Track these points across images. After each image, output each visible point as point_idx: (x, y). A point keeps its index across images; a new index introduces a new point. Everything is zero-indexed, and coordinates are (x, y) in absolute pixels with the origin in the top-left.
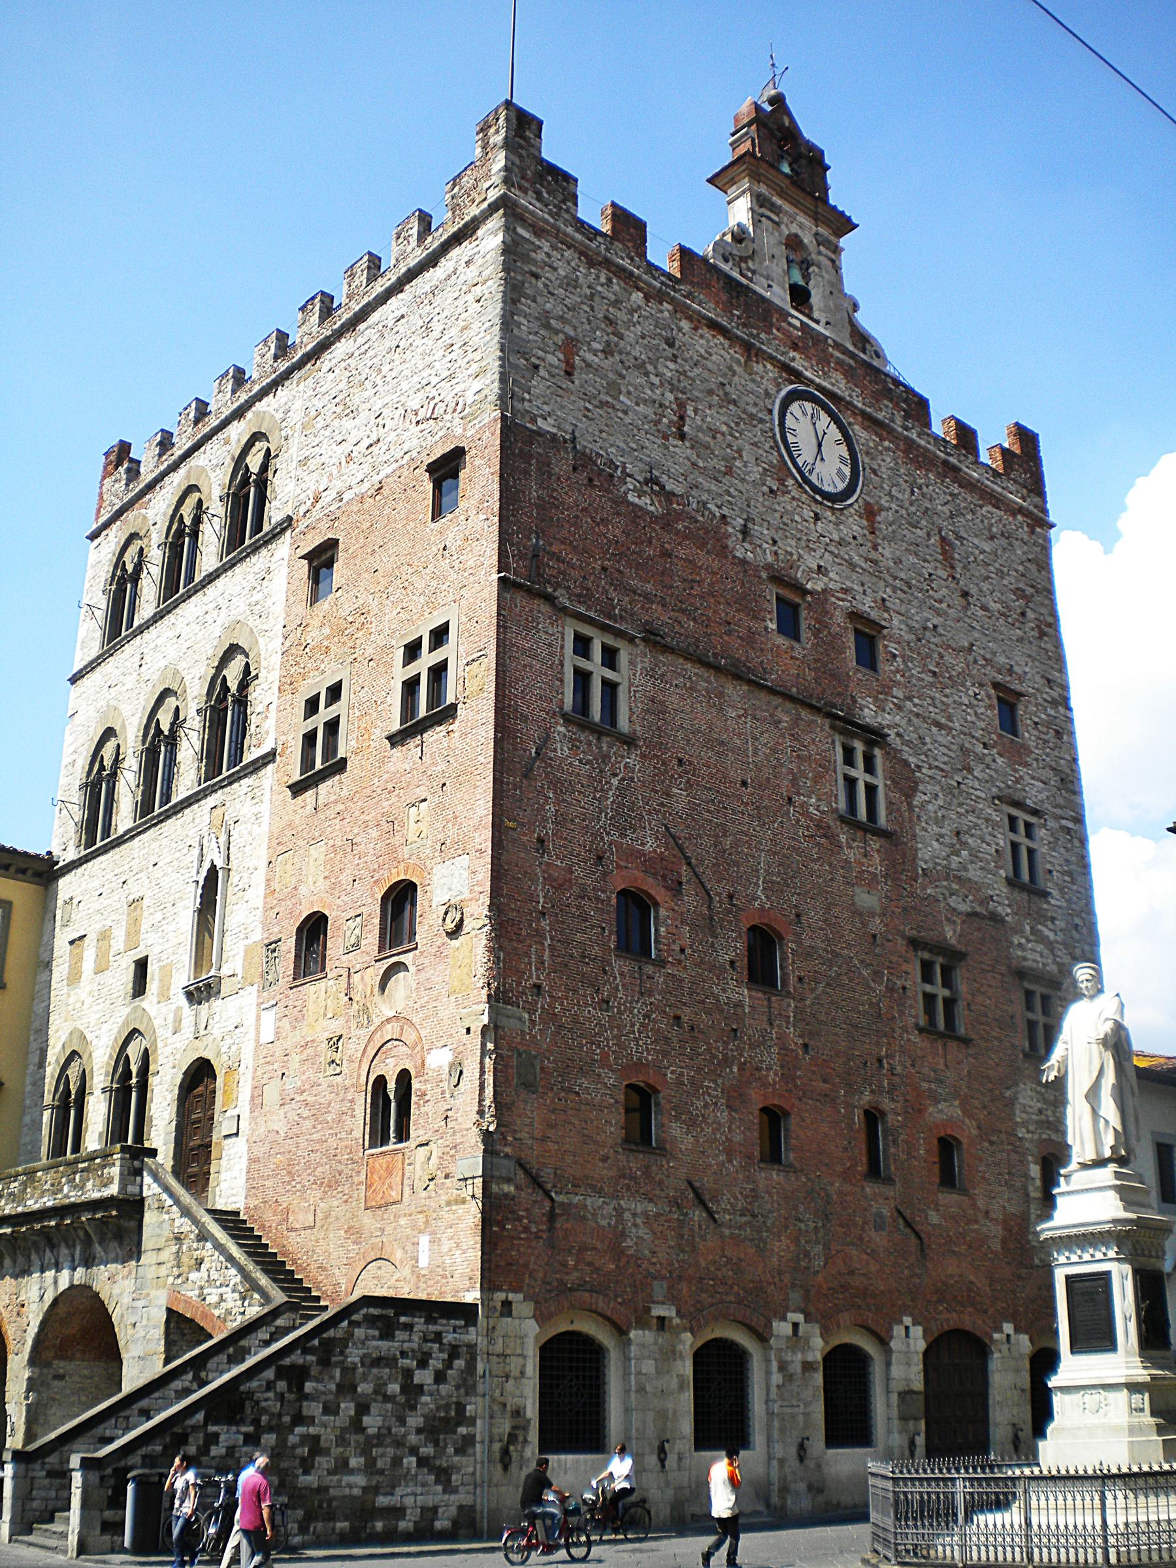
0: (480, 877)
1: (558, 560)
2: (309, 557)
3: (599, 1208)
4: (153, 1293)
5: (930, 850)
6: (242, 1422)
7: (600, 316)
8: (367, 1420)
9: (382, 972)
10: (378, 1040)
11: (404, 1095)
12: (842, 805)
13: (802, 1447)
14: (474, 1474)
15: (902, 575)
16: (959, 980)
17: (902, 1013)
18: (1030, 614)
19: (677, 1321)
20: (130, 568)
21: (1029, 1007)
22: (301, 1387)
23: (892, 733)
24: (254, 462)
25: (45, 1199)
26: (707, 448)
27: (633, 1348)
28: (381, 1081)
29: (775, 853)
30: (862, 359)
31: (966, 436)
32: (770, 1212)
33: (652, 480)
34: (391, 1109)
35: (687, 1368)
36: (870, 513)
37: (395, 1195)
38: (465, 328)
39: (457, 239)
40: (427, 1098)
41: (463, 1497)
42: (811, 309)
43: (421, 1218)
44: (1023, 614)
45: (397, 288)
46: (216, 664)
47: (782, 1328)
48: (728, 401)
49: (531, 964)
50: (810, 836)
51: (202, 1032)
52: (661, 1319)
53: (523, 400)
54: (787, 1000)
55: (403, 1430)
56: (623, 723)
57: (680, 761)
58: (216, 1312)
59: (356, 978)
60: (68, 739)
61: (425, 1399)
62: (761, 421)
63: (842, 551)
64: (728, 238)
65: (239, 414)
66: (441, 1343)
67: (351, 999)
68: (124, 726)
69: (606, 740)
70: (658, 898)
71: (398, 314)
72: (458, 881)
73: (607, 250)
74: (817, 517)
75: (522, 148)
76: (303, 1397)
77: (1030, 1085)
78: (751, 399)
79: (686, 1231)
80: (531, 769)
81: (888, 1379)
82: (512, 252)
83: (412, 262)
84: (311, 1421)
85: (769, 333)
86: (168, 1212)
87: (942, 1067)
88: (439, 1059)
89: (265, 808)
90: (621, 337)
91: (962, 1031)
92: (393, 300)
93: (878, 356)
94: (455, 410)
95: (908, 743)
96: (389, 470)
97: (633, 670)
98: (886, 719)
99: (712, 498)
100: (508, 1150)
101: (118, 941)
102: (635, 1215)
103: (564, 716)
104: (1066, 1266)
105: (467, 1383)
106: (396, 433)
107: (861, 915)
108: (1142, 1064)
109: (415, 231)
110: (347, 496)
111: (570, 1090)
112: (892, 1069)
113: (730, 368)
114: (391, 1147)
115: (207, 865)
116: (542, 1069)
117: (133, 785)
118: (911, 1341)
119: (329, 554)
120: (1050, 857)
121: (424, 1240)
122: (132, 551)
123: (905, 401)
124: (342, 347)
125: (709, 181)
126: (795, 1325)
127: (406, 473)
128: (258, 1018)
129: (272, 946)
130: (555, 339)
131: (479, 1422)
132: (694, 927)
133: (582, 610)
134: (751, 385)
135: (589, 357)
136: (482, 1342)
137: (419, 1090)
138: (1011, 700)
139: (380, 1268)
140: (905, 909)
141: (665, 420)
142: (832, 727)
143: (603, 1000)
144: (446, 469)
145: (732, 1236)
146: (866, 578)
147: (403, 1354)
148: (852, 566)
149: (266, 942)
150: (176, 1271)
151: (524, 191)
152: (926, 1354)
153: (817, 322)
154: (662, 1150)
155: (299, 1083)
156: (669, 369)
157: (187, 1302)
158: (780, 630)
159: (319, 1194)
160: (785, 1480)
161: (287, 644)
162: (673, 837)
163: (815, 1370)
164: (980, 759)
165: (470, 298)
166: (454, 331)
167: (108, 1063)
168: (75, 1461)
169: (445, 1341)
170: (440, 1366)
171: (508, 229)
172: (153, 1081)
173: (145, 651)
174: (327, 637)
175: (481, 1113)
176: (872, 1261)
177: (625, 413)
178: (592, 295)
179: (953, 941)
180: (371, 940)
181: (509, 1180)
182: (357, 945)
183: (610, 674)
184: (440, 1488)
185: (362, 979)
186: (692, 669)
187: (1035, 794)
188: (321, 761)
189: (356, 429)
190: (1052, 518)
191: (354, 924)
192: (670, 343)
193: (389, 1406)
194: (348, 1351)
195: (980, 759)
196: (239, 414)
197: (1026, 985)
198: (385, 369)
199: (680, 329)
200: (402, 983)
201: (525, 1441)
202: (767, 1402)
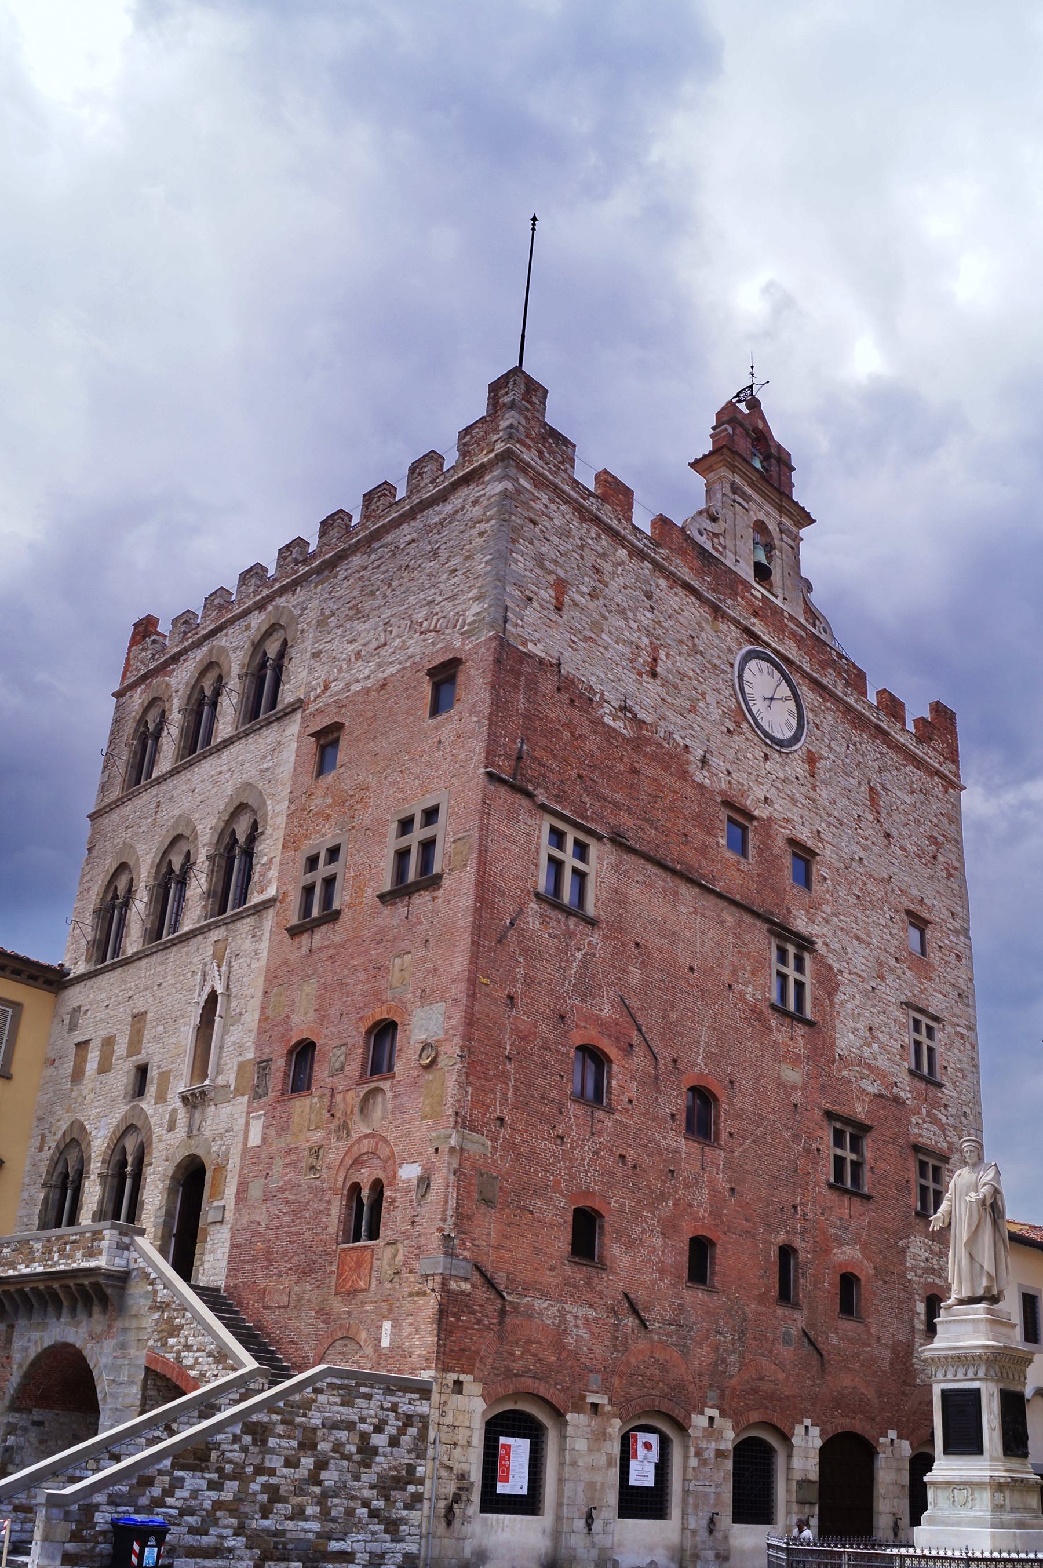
1: (539, 764)
3: (545, 1309)
6: (207, 1469)
9: (362, 1094)
11: (376, 1201)
13: (712, 1521)
16: (865, 1148)
17: (815, 1170)
19: (608, 1408)
27: (569, 1428)
29: (715, 1029)
32: (694, 1323)
40: (397, 1204)
49: (495, 1099)
50: (746, 1019)
52: (595, 1406)
54: (718, 1152)
58: (192, 1373)
59: (339, 1098)
66: (396, 1412)
67: (333, 1115)
70: (612, 1056)
77: (919, 1238)
79: (620, 1334)
80: (506, 937)
81: (789, 1469)
87: (847, 1217)
88: (410, 1172)
91: (866, 1190)
97: (600, 860)
99: (676, 728)
100: (466, 1253)
102: (576, 1317)
107: (785, 1087)
108: (1014, 1229)
111: (524, 1209)
116: (501, 1188)
118: (810, 1439)
130: (548, 578)
132: (642, 1084)
133: (559, 808)
135: (577, 597)
137: (390, 1197)
140: (822, 1086)
143: (558, 1136)
145: (660, 1342)
150: (156, 1336)
155: (281, 1183)
157: (165, 1362)
159: (294, 1278)
160: (696, 1548)
163: (726, 1457)
169: (400, 1411)
170: (395, 1432)
175: (444, 1220)
176: (779, 1370)
177: (606, 649)
180: (354, 1068)
200: (380, 1106)
202: (684, 1480)
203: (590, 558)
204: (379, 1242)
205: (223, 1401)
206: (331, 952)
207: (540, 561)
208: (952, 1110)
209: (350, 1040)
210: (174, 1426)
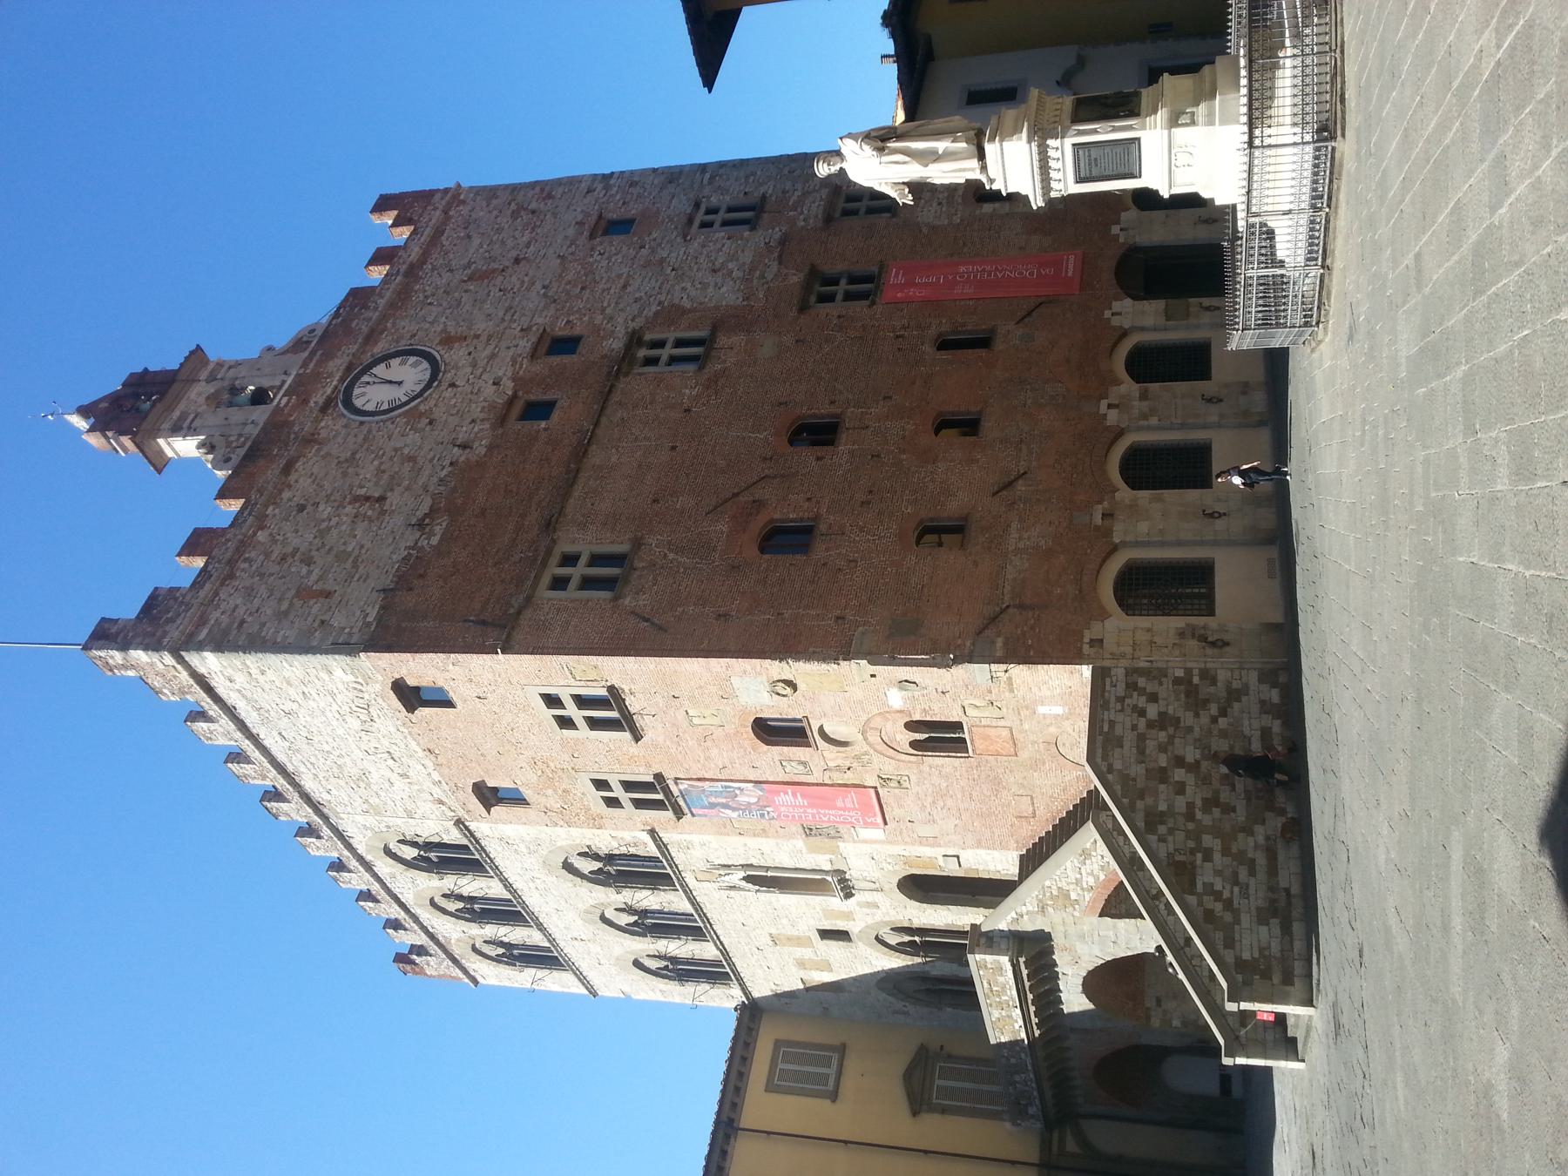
0: (749, 668)
2: (488, 809)
5: (727, 295)
7: (277, 568)
8: (1190, 759)
12: (690, 368)
13: (1210, 400)
14: (1232, 670)
15: (501, 314)
18: (533, 206)
20: (501, 951)
21: (855, 212)
22: (1162, 814)
23: (632, 325)
24: (410, 853)
26: (392, 477)
28: (915, 745)
30: (317, 344)
31: (382, 256)
33: (420, 525)
34: (939, 737)
35: (1144, 495)
36: (448, 341)
37: (1005, 733)
38: (289, 683)
39: (209, 690)
41: (1253, 678)
42: (272, 388)
43: (1024, 713)
44: (533, 212)
47: (1113, 417)
48: (352, 460)
53: (350, 634)
55: (1197, 729)
56: (623, 548)
57: (655, 501)
58: (1102, 877)
59: (831, 764)
60: (642, 996)
61: (1171, 711)
62: (369, 431)
63: (481, 363)
64: (210, 457)
65: (368, 867)
68: (631, 953)
69: (638, 564)
71: (278, 738)
72: (752, 684)
73: (219, 562)
74: (453, 385)
75: (125, 637)
76: (1171, 811)
78: (351, 439)
81: (1155, 329)
82: (221, 644)
83: (232, 727)
84: (1190, 806)
85: (293, 424)
88: (896, 698)
89: (696, 838)
90: (296, 550)
92: (266, 743)
93: (313, 331)
95: (641, 312)
96: (413, 745)
98: (621, 331)
101: (806, 953)
103: (615, 599)
104: (1066, 184)
105: (1158, 674)
109: (204, 725)
110: (436, 776)
112: (904, 328)
113: (323, 457)
114: (966, 736)
115: (743, 883)
117: (679, 942)
120: (734, 192)
121: (1041, 710)
122: (487, 949)
123: (352, 309)
124: (309, 784)
125: (159, 471)
126: (1110, 406)
128: (865, 842)
131: (1190, 665)
134: (340, 440)
135: (314, 577)
136: (1124, 663)
138: (603, 224)
141: (370, 513)
142: (627, 374)
144: (411, 697)
146: (503, 344)
147: (1134, 727)
148: (493, 356)
151: (165, 634)
152: (1135, 298)
153: (284, 382)
154: (965, 519)
156: (325, 510)
157: (1094, 900)
158: (546, 417)
162: (716, 508)
163: (1146, 390)
164: (653, 251)
165: (261, 679)
166: (292, 691)
168: (1231, 1007)
170: (1143, 699)
171: (200, 648)
172: (916, 924)
178: (262, 575)
179: (801, 275)
181: (993, 642)
182: (804, 764)
183: (583, 560)
184: (1244, 699)
186: (577, 492)
187: (682, 205)
188: (652, 794)
189: (379, 771)
190: (451, 185)
192: (301, 508)
193: (1177, 741)
194: (1133, 774)
195: (653, 251)
196: (368, 867)
197: (837, 214)
198: (327, 748)
199: (290, 500)
201: (1204, 627)
203: (275, 568)
204: (964, 720)
205: (1126, 849)
207: (282, 616)
208: (788, 185)
209: (777, 758)
210: (1154, 892)
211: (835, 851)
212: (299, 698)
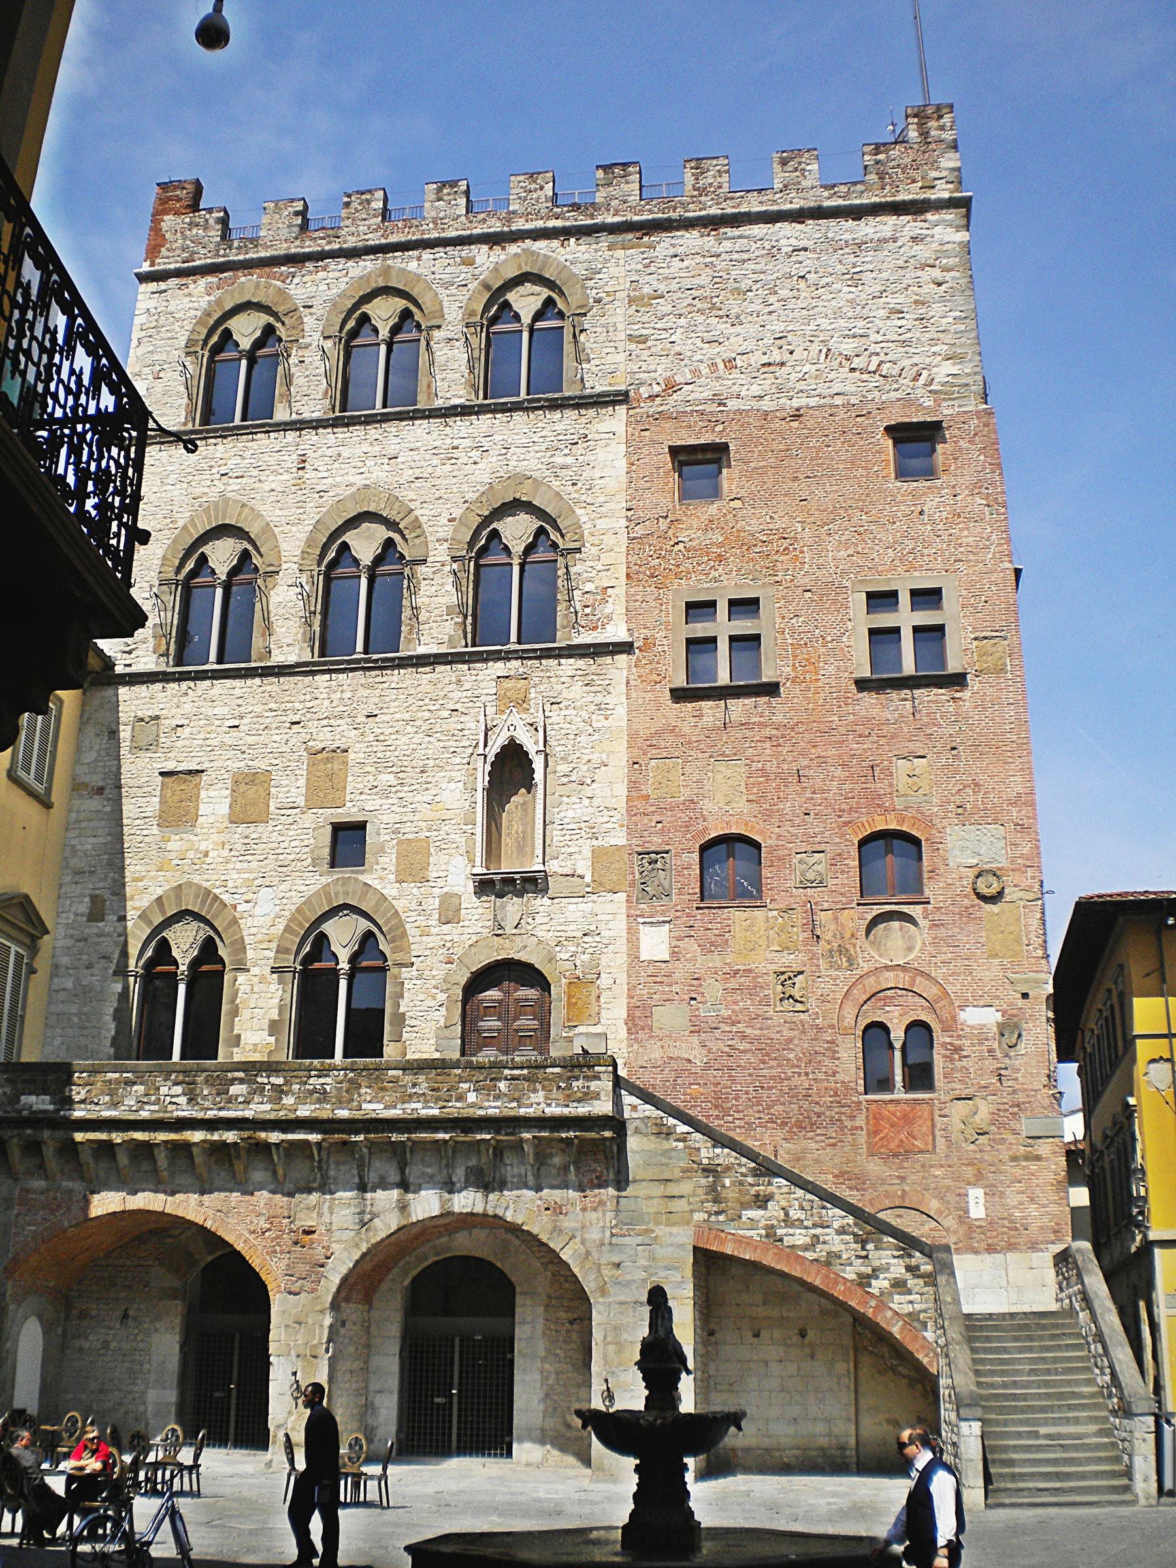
4: (660, 1230)
10: (871, 984)
25: (414, 1106)
38: (916, 302)
39: (897, 208)
43: (969, 1172)
45: (798, 216)
46: (486, 513)
51: (509, 930)
58: (810, 1255)
86: (684, 1140)
88: (981, 1017)
89: (618, 701)
94: (915, 379)
96: (813, 402)
106: (814, 367)
110: (732, 404)
119: (709, 456)
124: (691, 239)
127: (841, 414)
129: (652, 857)
139: (900, 1216)
149: (640, 849)
157: (740, 1241)
161: (639, 531)
167: (281, 937)
173: (310, 453)
174: (720, 545)
185: (836, 918)
191: (811, 861)
198: (784, 293)
206: (768, 732)
211: (599, 887)
212: (893, 301)
